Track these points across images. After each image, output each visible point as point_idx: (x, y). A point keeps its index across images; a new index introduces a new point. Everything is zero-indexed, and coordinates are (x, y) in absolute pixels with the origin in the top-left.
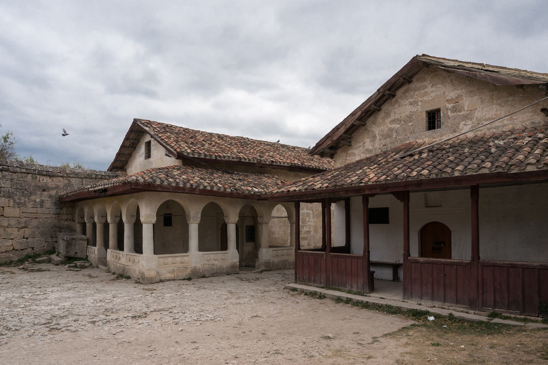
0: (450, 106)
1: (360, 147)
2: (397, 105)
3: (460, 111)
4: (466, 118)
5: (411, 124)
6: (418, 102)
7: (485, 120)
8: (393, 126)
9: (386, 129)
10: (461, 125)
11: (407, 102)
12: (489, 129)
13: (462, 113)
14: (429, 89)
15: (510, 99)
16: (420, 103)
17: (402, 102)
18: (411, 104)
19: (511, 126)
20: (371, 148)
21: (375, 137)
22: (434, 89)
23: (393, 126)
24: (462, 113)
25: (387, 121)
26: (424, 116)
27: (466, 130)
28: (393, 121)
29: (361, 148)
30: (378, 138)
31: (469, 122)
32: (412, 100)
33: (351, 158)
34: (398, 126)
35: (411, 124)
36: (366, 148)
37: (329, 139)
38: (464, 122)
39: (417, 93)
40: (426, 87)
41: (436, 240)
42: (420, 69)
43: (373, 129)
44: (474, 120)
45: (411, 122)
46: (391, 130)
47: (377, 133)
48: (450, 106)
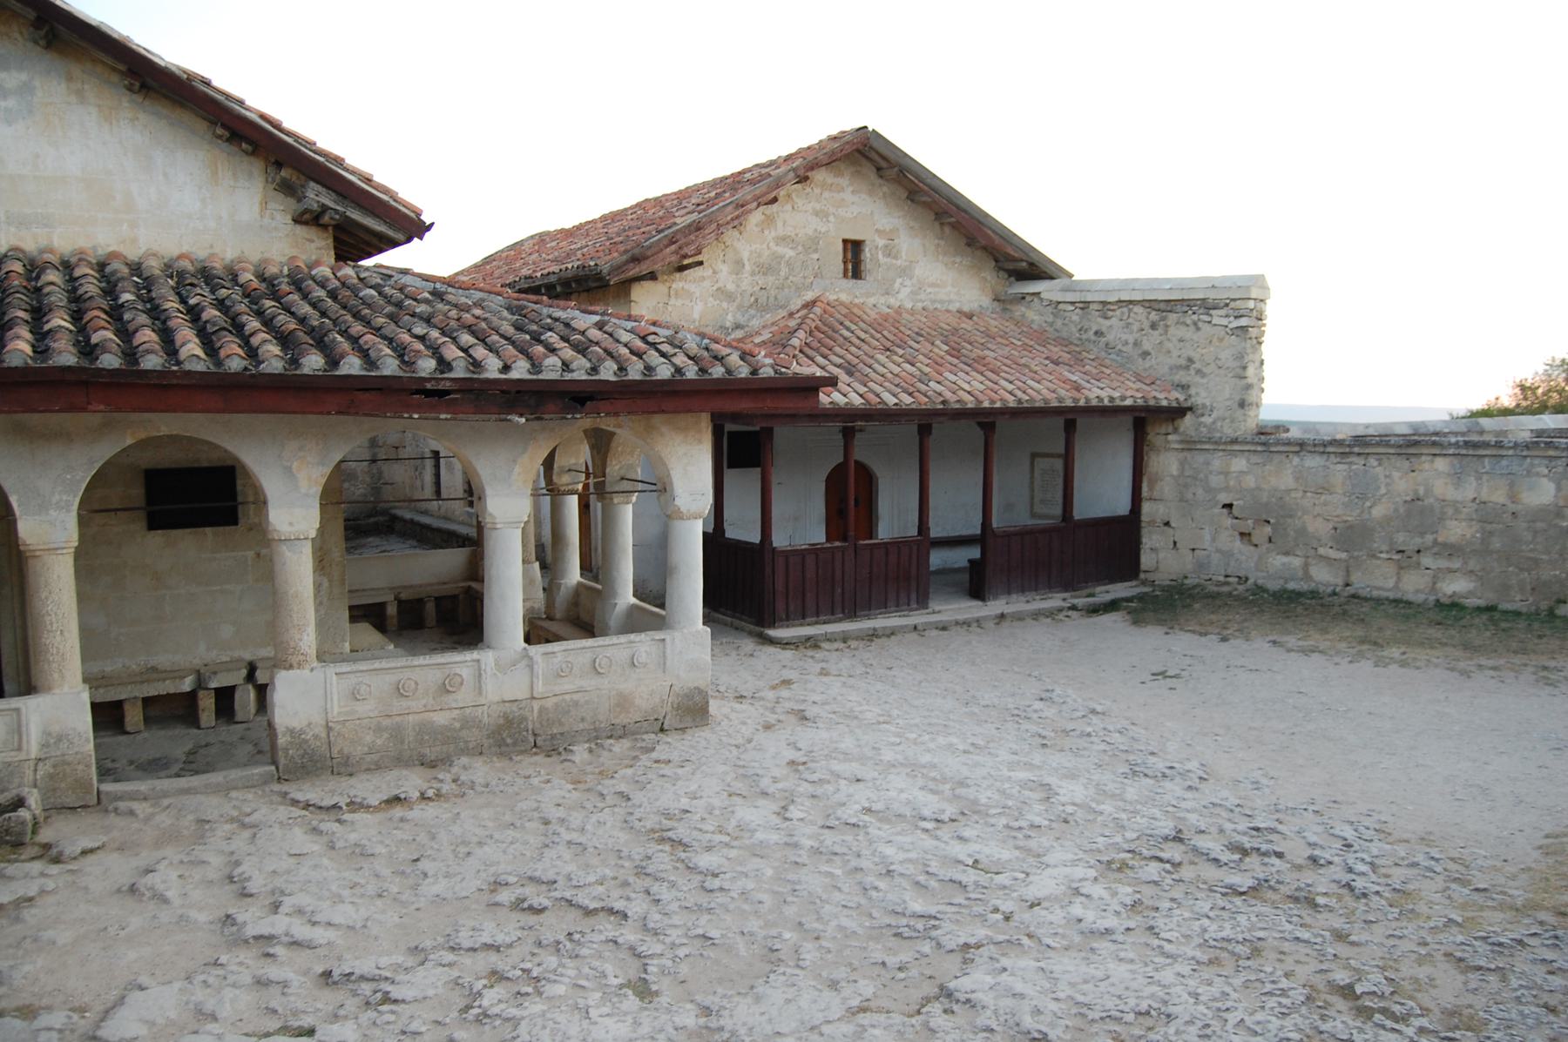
0: (881, 242)
1: (703, 278)
2: (788, 207)
3: (896, 258)
4: (905, 272)
5: (816, 256)
6: (827, 215)
7: (932, 285)
8: (780, 250)
9: (767, 253)
10: (897, 285)
11: (810, 207)
12: (934, 301)
13: (899, 262)
14: (847, 195)
15: (958, 260)
16: (832, 218)
17: (799, 202)
18: (816, 213)
19: (957, 305)
20: (731, 287)
21: (739, 263)
22: (855, 198)
23: (780, 250)
24: (899, 262)
25: (770, 235)
26: (840, 246)
27: (903, 296)
28: (782, 240)
29: (707, 283)
30: (748, 267)
31: (908, 283)
32: (818, 206)
33: (679, 303)
34: (791, 253)
35: (816, 256)
36: (720, 284)
37: (673, 247)
38: (899, 281)
39: (826, 194)
40: (843, 190)
41: (850, 498)
42: (865, 156)
43: (738, 245)
44: (915, 280)
45: (816, 251)
46: (778, 258)
47: (745, 255)
48: (881, 242)
